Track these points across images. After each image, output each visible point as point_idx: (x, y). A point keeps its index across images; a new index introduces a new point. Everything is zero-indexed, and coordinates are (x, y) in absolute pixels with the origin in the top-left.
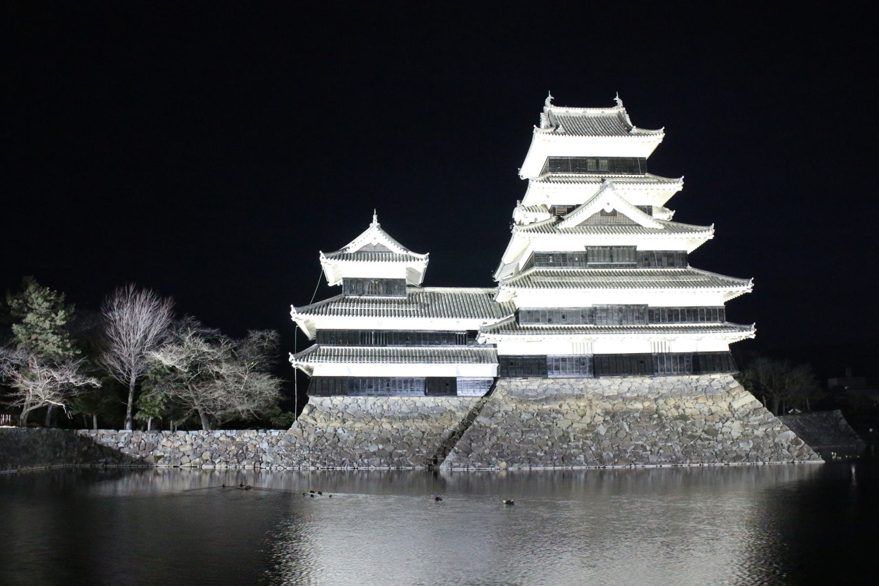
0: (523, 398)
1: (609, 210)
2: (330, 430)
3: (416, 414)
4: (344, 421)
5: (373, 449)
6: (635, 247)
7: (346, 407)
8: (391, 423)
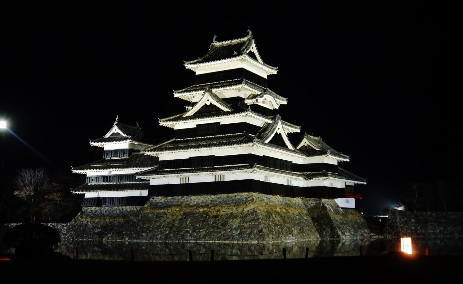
0: (155, 206)
1: (208, 104)
2: (85, 223)
3: (121, 215)
4: (92, 218)
5: (97, 231)
6: (220, 123)
7: (96, 211)
8: (109, 219)
